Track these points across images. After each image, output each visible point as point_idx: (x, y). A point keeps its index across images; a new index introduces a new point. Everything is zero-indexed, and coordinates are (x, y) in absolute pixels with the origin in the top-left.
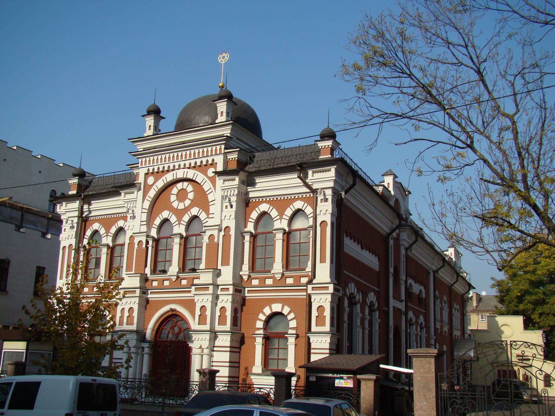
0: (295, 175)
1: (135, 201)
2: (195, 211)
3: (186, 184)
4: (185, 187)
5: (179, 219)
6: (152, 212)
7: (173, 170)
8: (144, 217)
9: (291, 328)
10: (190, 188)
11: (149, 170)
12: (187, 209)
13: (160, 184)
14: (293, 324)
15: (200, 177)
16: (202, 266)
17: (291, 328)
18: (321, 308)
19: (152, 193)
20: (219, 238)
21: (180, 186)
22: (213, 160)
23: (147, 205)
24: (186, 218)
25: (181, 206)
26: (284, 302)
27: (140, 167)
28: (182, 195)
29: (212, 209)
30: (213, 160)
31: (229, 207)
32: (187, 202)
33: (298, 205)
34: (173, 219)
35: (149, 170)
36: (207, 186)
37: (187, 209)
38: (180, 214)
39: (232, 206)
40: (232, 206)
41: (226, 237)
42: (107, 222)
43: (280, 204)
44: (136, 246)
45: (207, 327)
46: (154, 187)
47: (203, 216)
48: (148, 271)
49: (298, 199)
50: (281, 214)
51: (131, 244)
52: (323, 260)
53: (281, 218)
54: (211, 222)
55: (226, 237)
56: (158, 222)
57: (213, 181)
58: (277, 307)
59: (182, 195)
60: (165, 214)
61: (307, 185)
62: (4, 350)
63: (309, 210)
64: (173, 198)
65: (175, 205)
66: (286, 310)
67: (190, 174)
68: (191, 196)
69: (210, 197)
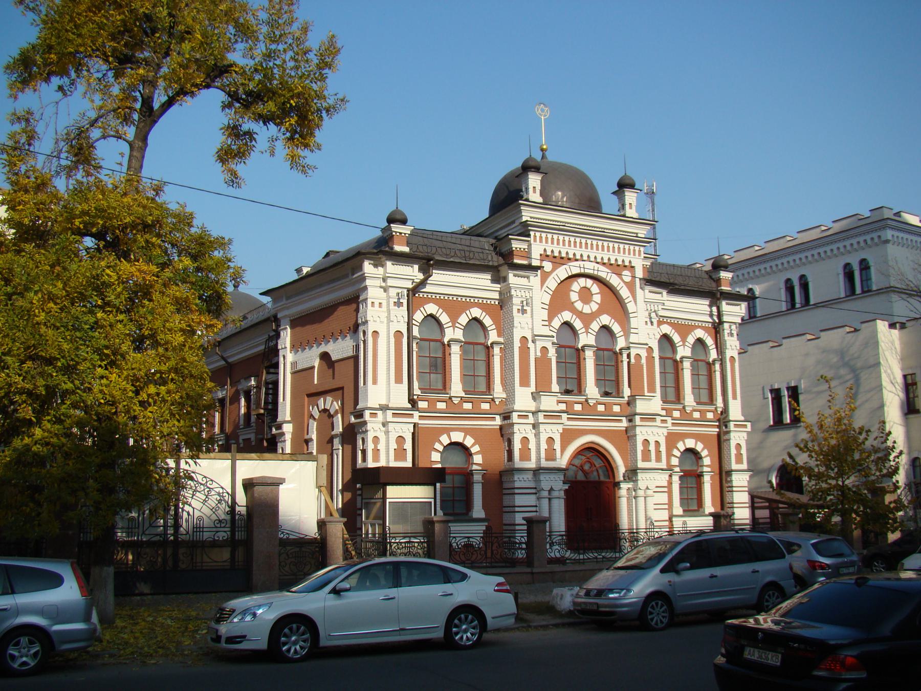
0: (707, 302)
1: (530, 290)
2: (605, 319)
3: (589, 282)
4: (588, 286)
5: (587, 326)
6: (554, 309)
7: (577, 260)
8: (545, 315)
9: (707, 466)
10: (595, 289)
11: (545, 250)
12: (593, 316)
13: (562, 273)
14: (707, 461)
15: (614, 280)
16: (627, 392)
17: (707, 466)
18: (738, 446)
19: (552, 283)
20: (644, 361)
21: (582, 281)
22: (630, 262)
23: (547, 299)
24: (595, 326)
25: (587, 310)
26: (697, 437)
27: (532, 242)
28: (585, 295)
29: (634, 323)
30: (630, 262)
31: (649, 323)
32: (595, 307)
33: (700, 333)
34: (578, 324)
35: (545, 250)
36: (624, 293)
37: (593, 316)
38: (587, 319)
39: (652, 322)
40: (652, 322)
41: (650, 359)
42: (454, 306)
43: (684, 329)
44: (534, 352)
45: (663, 465)
46: (554, 275)
47: (616, 328)
48: (555, 387)
49: (699, 327)
50: (684, 340)
51: (524, 350)
52: (735, 398)
53: (684, 345)
54: (633, 338)
55: (650, 359)
56: (556, 323)
57: (631, 286)
58: (690, 443)
59: (585, 295)
60: (567, 316)
61: (720, 315)
62: (388, 501)
63: (710, 341)
64: (574, 297)
65: (579, 305)
66: (699, 447)
67: (603, 273)
68: (597, 298)
69: (631, 307)
